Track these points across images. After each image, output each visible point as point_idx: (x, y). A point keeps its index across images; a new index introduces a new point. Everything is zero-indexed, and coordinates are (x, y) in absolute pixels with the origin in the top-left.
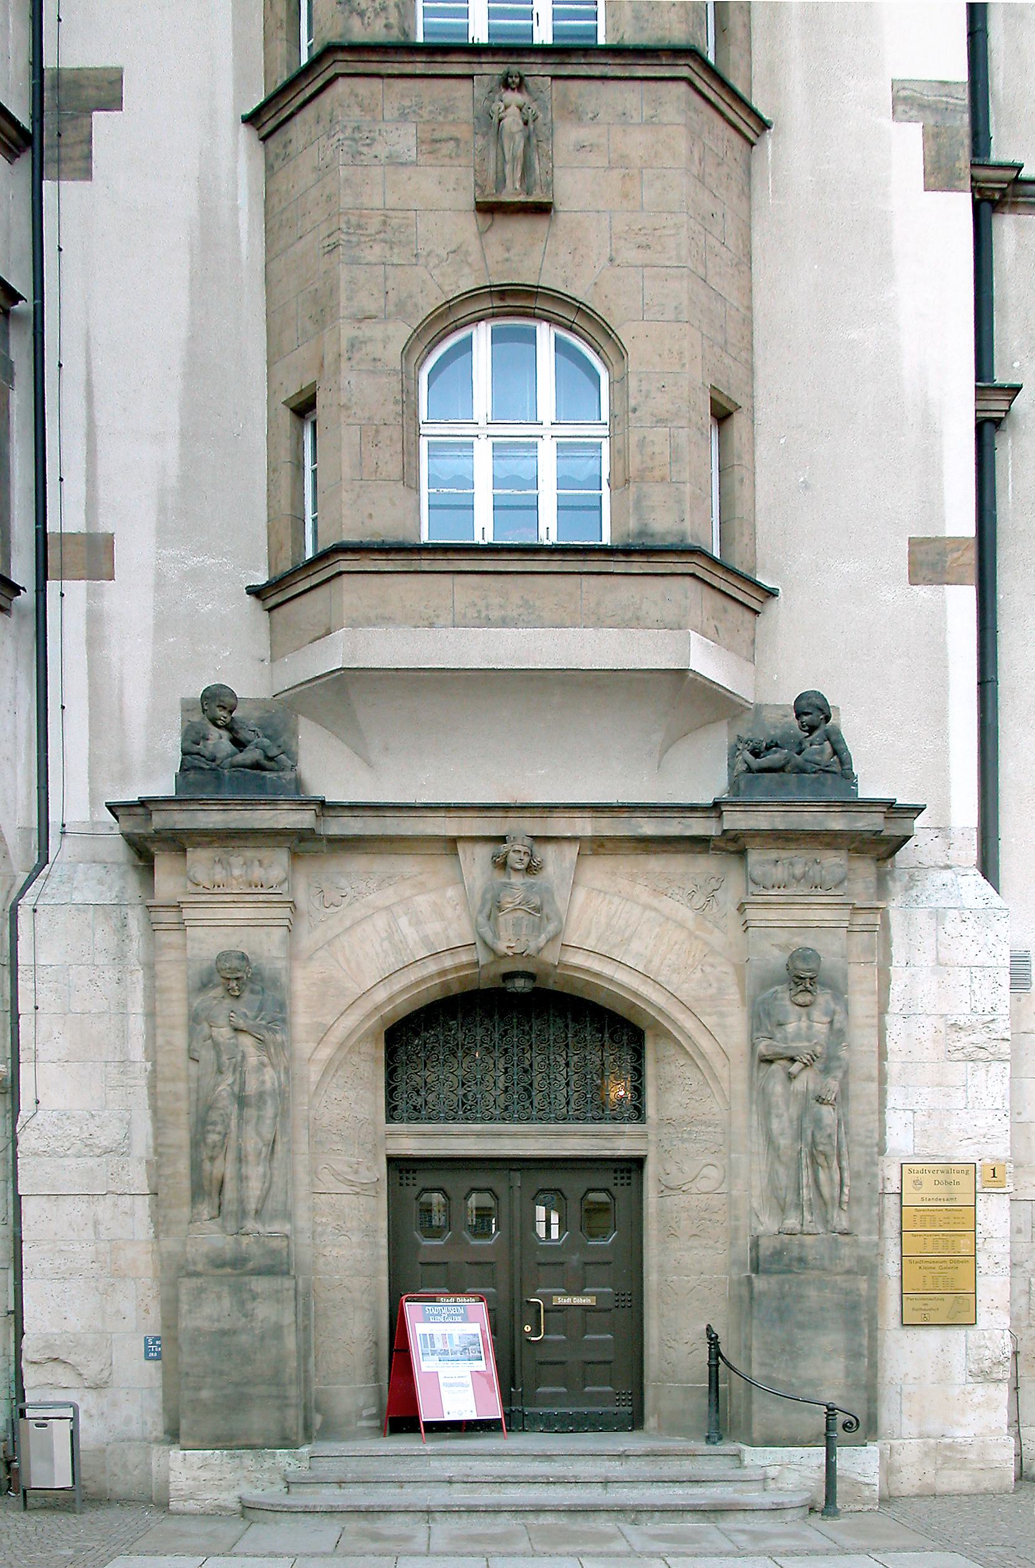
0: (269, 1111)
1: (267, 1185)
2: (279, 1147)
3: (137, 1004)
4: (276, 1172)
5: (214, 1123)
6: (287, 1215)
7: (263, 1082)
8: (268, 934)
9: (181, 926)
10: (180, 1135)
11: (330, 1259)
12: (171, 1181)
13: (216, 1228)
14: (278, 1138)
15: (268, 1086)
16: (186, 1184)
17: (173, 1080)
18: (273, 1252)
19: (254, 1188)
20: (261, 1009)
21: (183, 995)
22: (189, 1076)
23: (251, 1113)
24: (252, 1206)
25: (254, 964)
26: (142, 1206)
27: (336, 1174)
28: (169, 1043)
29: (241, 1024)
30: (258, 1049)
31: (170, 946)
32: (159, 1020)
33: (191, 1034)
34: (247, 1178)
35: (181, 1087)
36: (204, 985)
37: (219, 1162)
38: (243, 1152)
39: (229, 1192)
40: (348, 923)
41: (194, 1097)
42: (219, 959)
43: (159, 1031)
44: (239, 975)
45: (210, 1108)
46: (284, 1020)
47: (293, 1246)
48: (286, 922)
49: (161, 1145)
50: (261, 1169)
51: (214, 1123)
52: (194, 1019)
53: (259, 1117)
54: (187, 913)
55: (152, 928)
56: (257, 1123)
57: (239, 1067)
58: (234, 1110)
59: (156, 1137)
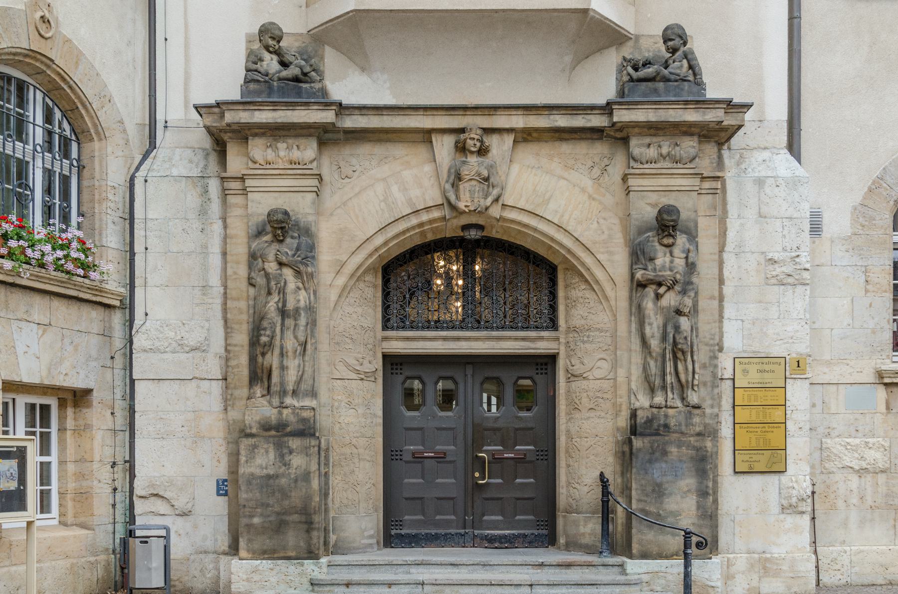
0: (302, 321)
1: (300, 373)
2: (309, 346)
3: (215, 248)
4: (307, 364)
5: (265, 329)
6: (313, 394)
7: (299, 301)
8: (303, 197)
9: (245, 192)
10: (242, 338)
11: (343, 425)
12: (236, 370)
13: (265, 403)
14: (309, 340)
15: (302, 304)
16: (245, 372)
17: (238, 299)
18: (304, 420)
19: (292, 376)
20: (298, 249)
21: (246, 240)
22: (248, 296)
23: (289, 322)
24: (290, 387)
25: (293, 218)
26: (216, 388)
27: (347, 365)
28: (235, 273)
29: (284, 259)
30: (296, 277)
31: (236, 205)
32: (229, 258)
33: (250, 267)
34: (287, 368)
35: (243, 305)
36: (259, 233)
37: (268, 356)
38: (285, 350)
39: (275, 379)
40: (357, 190)
41: (251, 311)
42: (269, 215)
43: (229, 265)
44: (283, 225)
45: (262, 319)
46: (313, 257)
47: (318, 417)
48: (315, 189)
49: (230, 345)
50: (297, 362)
51: (265, 329)
52: (253, 257)
53: (296, 325)
54: (248, 183)
55: (225, 194)
56: (294, 329)
57: (282, 291)
58: (278, 320)
59: (226, 340)
